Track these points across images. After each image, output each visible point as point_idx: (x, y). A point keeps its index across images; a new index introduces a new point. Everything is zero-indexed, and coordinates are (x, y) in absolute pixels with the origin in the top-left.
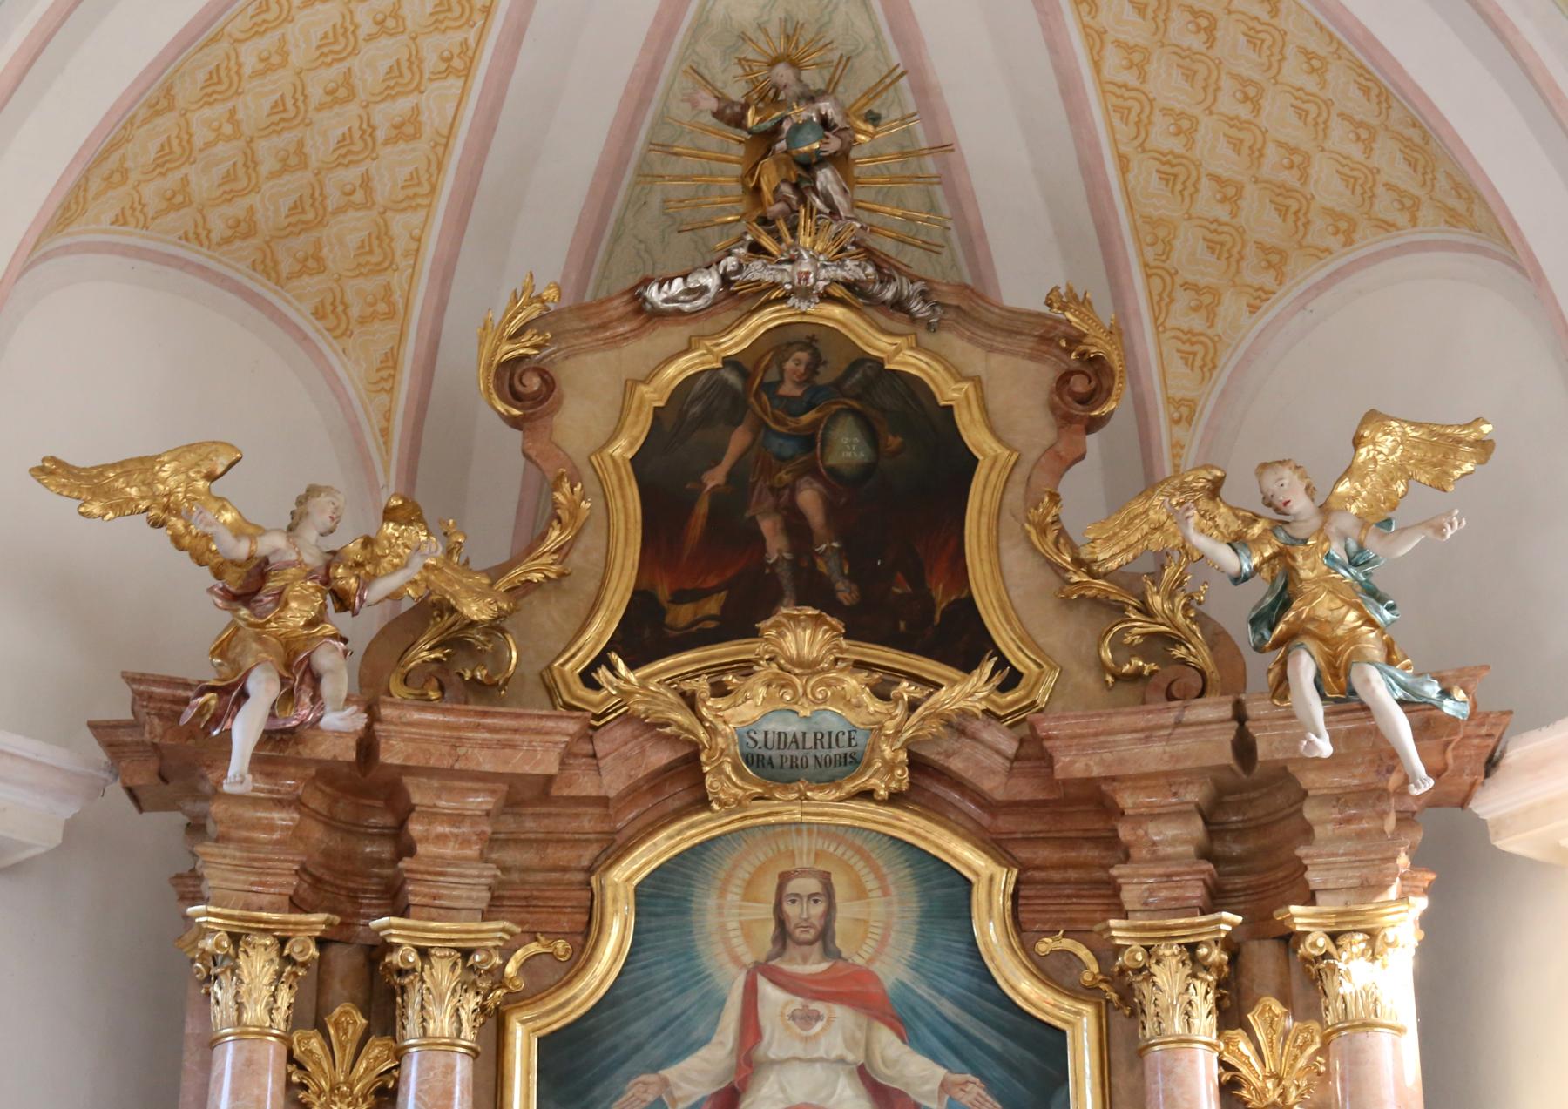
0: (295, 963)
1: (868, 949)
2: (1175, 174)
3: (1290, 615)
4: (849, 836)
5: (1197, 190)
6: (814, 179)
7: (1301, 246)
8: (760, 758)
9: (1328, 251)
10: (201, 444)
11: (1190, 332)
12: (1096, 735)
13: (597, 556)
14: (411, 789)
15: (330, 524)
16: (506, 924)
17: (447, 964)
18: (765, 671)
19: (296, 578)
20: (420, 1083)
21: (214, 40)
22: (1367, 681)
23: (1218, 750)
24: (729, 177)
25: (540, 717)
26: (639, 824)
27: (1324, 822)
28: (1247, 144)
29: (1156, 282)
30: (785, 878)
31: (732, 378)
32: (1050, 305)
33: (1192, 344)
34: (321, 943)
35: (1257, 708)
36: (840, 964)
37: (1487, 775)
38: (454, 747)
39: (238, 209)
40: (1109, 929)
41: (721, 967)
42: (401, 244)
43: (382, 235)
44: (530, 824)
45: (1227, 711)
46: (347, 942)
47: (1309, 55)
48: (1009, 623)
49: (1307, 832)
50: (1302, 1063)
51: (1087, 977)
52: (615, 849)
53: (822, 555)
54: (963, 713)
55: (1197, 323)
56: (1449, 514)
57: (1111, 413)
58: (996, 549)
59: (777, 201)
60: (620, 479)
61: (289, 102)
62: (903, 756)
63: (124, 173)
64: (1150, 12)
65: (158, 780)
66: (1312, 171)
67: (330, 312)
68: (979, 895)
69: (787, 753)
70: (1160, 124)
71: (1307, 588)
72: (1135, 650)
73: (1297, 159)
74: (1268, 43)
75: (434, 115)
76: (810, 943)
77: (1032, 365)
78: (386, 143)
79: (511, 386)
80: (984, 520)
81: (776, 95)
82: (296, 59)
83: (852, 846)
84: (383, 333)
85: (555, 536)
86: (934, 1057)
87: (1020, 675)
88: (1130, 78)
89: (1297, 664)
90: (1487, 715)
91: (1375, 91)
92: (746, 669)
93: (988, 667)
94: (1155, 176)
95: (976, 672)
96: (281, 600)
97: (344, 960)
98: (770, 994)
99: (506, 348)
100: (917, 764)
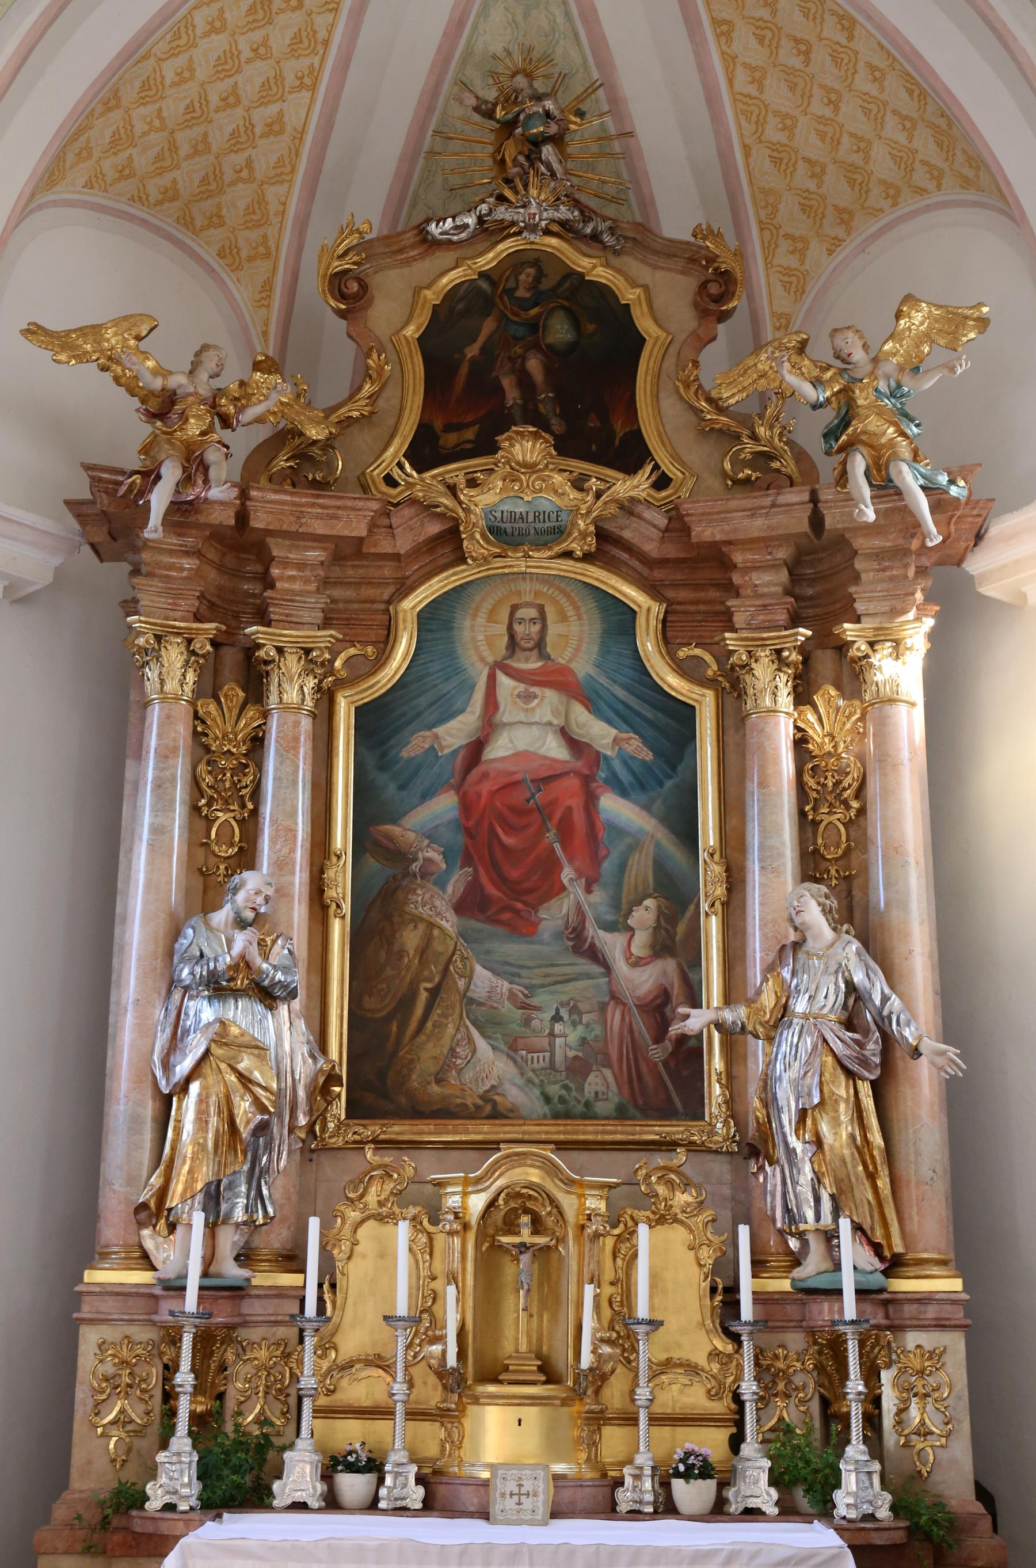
0: (197, 655)
1: (568, 653)
3: (850, 430)
4: (557, 582)
5: (795, 170)
6: (540, 152)
7: (863, 208)
8: (499, 529)
9: (882, 210)
10: (132, 316)
11: (788, 268)
12: (719, 513)
13: (395, 402)
14: (272, 546)
15: (216, 369)
16: (333, 632)
17: (295, 658)
18: (503, 470)
19: (193, 403)
20: (278, 732)
21: (145, 58)
22: (900, 472)
23: (799, 522)
24: (484, 154)
25: (355, 499)
26: (420, 573)
27: (867, 571)
28: (829, 135)
29: (767, 233)
30: (514, 608)
31: (485, 285)
32: (695, 236)
33: (790, 276)
34: (214, 643)
35: (826, 495)
36: (550, 663)
37: (975, 545)
38: (299, 518)
39: (166, 180)
40: (725, 639)
41: (473, 664)
42: (273, 207)
43: (261, 200)
44: (350, 572)
45: (806, 497)
46: (232, 645)
47: (872, 68)
48: (664, 446)
49: (856, 578)
50: (848, 726)
51: (710, 673)
52: (405, 589)
53: (542, 401)
54: (633, 500)
55: (792, 261)
56: (960, 359)
57: (735, 308)
58: (656, 397)
59: (515, 166)
60: (410, 351)
61: (197, 105)
62: (592, 528)
63: (88, 148)
64: (767, 42)
65: (109, 538)
66: (873, 154)
67: (228, 252)
68: (641, 621)
69: (516, 525)
70: (772, 122)
71: (862, 411)
72: (745, 464)
73: (863, 145)
74: (845, 61)
75: (293, 120)
76: (531, 650)
77: (682, 278)
78: (261, 137)
79: (340, 290)
80: (649, 378)
81: (516, 98)
82: (201, 74)
83: (558, 588)
84: (263, 267)
85: (368, 388)
86: (610, 723)
87: (671, 480)
88: (752, 90)
89: (853, 462)
90: (978, 502)
91: (916, 93)
93: (648, 468)
94: (768, 159)
95: (641, 472)
96: (184, 418)
97: (231, 656)
98: (505, 682)
99: (336, 264)
100: (602, 535)
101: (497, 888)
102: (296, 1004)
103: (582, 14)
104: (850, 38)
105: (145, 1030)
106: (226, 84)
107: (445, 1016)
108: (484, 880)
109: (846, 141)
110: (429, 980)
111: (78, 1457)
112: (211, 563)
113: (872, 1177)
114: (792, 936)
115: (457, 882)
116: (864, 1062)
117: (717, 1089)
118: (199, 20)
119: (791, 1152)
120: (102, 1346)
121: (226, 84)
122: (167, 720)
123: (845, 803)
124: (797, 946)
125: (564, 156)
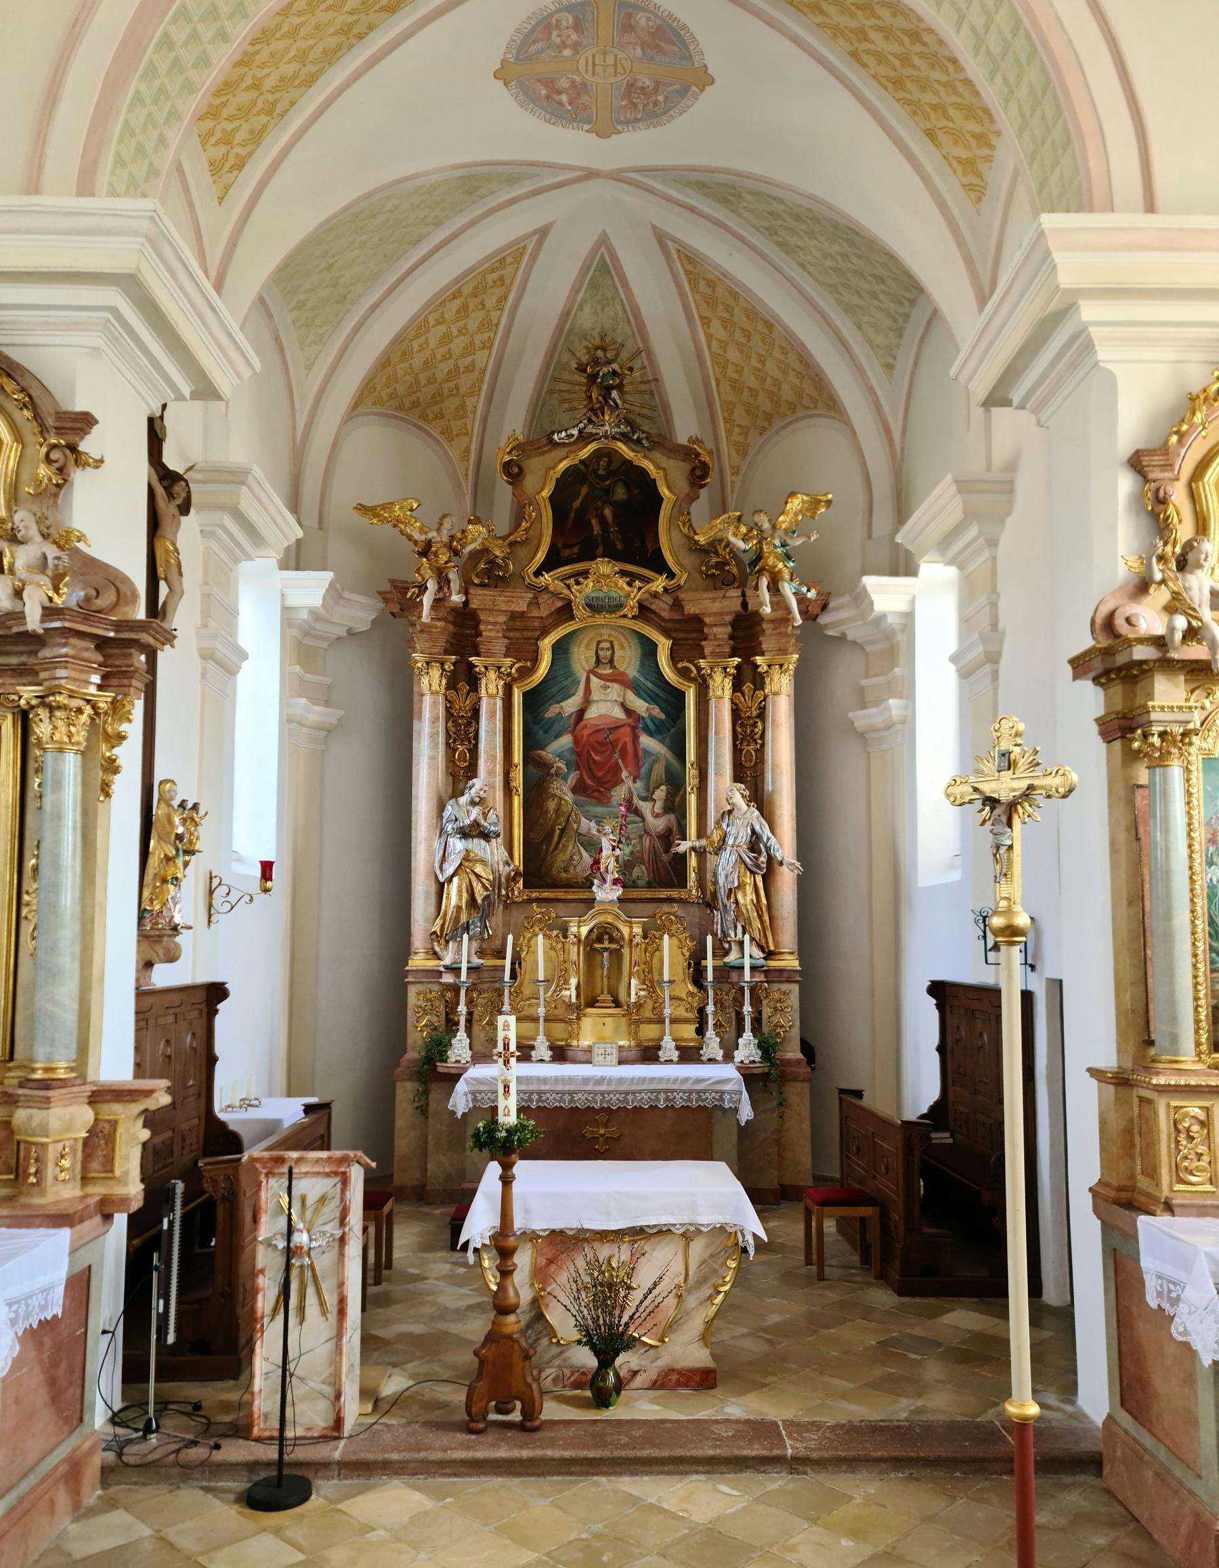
1: (624, 666)
2: (736, 386)
30: (599, 643)
31: (582, 467)
34: (454, 664)
35: (749, 592)
39: (414, 398)
42: (469, 408)
47: (782, 348)
52: (545, 632)
63: (374, 387)
67: (446, 432)
82: (432, 345)
88: (721, 352)
92: (585, 574)
100: (641, 606)
102: (500, 840)
103: (632, 311)
104: (771, 332)
105: (431, 853)
106: (445, 349)
109: (769, 381)
111: (410, 1040)
112: (450, 622)
113: (760, 917)
114: (729, 808)
115: (572, 779)
116: (758, 867)
117: (693, 875)
118: (432, 321)
119: (725, 906)
120: (418, 994)
121: (445, 349)
122: (435, 704)
123: (755, 741)
124: (730, 812)
125: (622, 393)
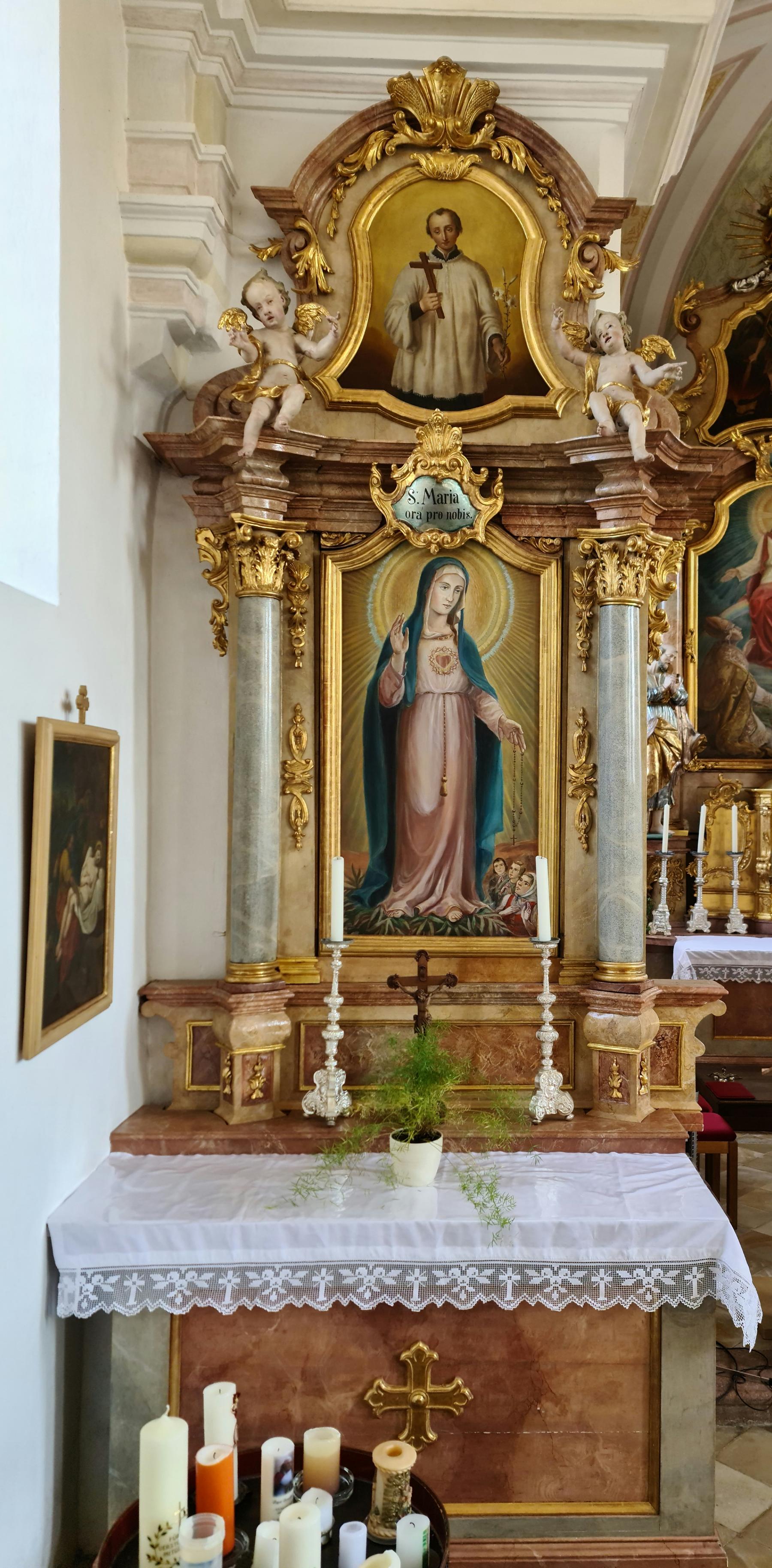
31: (759, 319)
52: (722, 493)
101: (768, 648)
107: (743, 710)
108: (762, 644)
110: (734, 693)
